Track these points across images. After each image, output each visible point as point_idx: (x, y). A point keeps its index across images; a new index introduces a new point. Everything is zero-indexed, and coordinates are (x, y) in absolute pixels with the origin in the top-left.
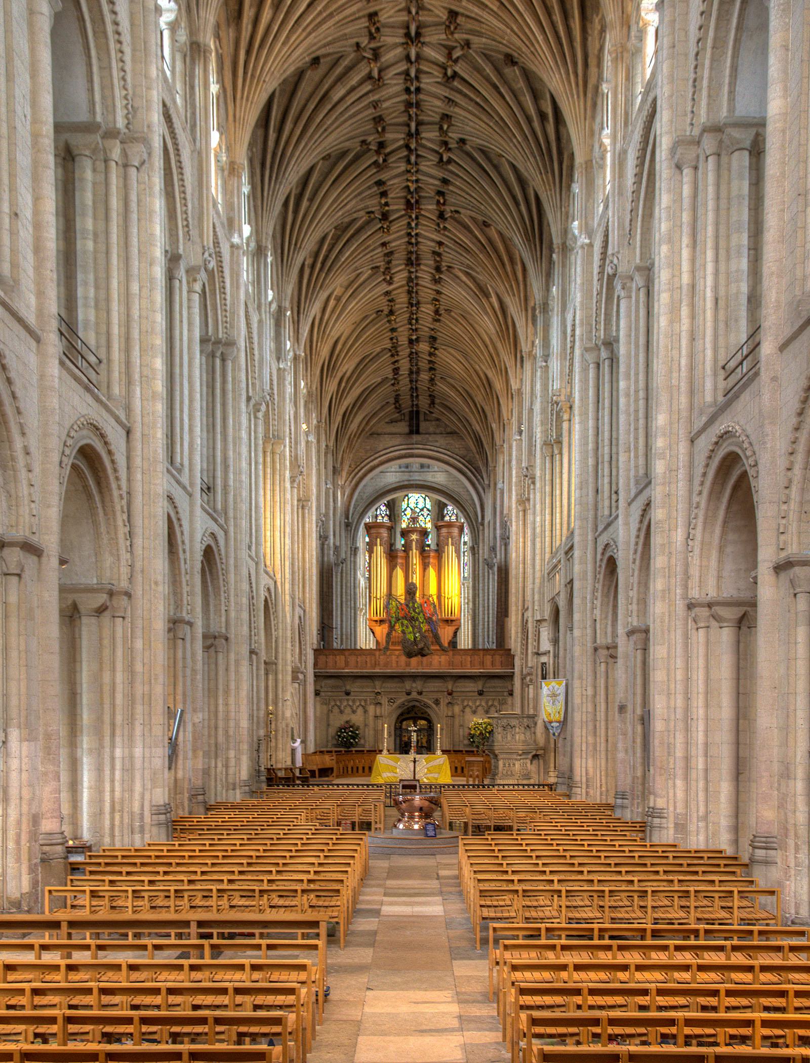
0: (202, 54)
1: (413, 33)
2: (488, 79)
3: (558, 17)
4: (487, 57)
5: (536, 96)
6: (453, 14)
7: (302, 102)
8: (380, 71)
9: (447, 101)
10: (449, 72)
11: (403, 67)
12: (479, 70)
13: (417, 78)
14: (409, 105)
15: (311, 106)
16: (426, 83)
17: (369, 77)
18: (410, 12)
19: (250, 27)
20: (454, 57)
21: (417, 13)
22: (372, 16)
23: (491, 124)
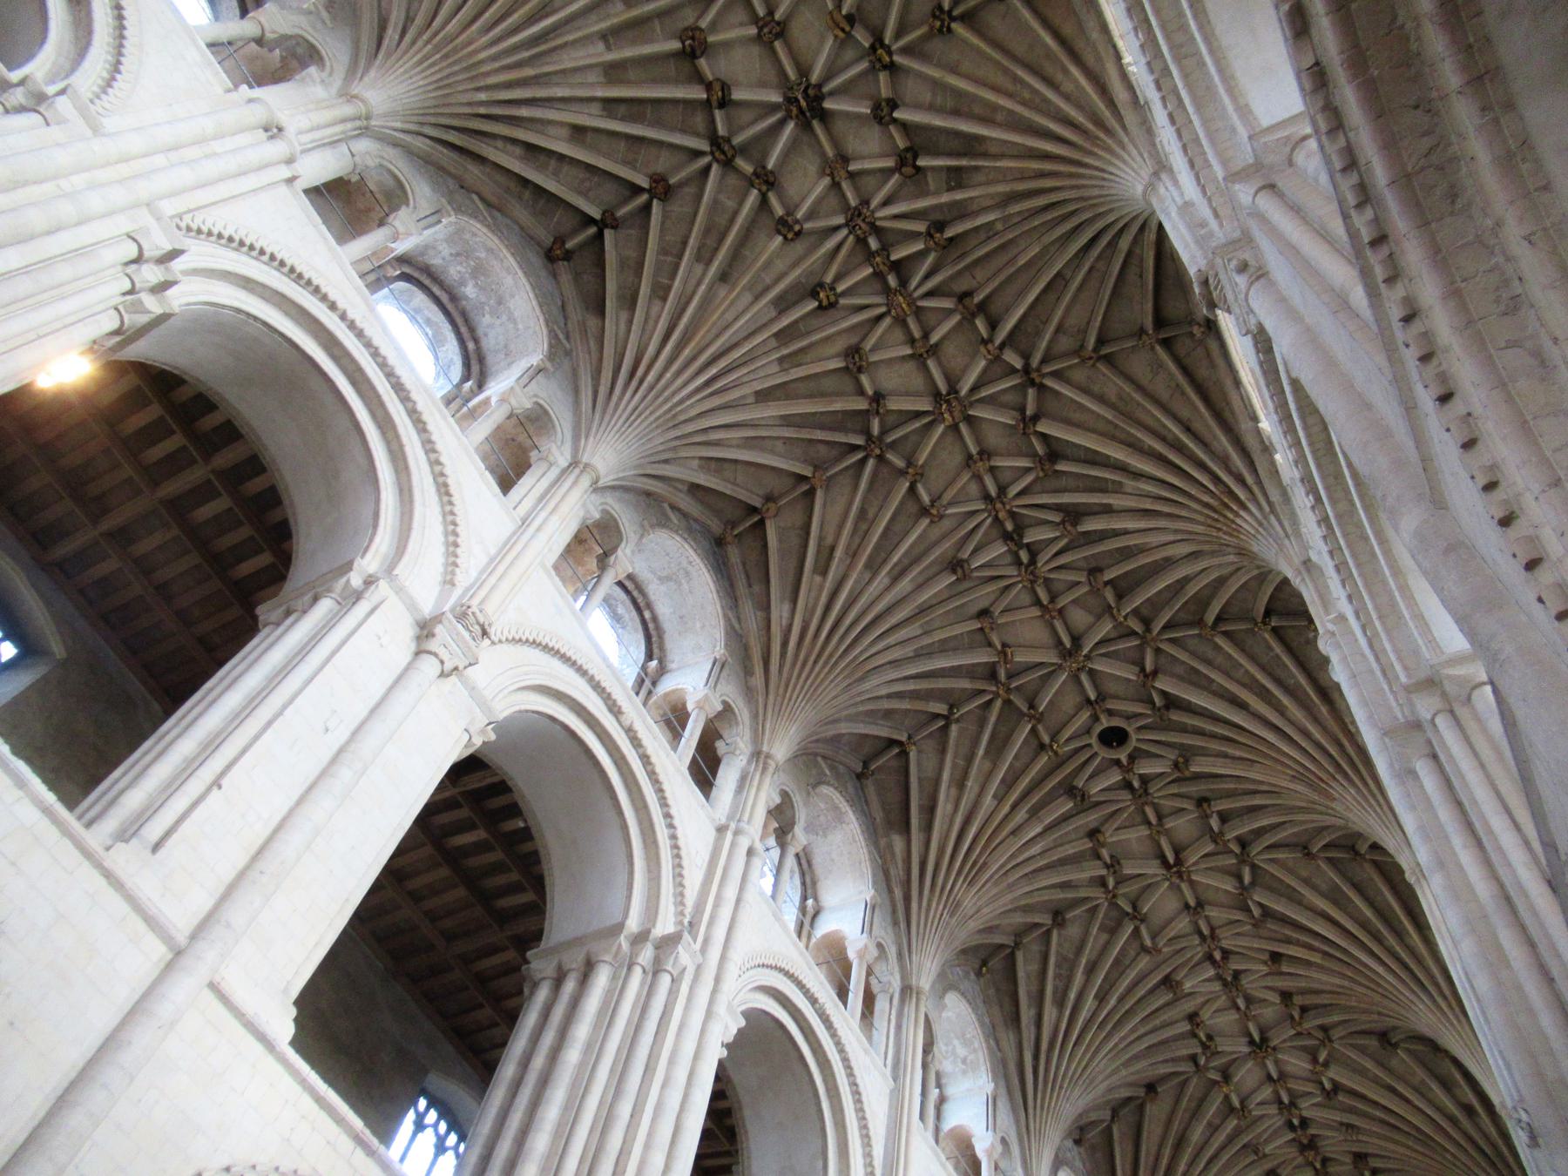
0: (914, 995)
1: (1257, 1038)
2: (1376, 1081)
3: (1391, 940)
4: (1362, 1050)
5: (1447, 1085)
6: (1286, 996)
7: (1154, 1150)
8: (1242, 1102)
9: (1344, 1129)
10: (1328, 1086)
11: (1266, 1092)
12: (1362, 1072)
13: (1293, 1104)
14: (1303, 1148)
15: (1167, 1152)
16: (1307, 1108)
17: (1229, 1110)
18: (1238, 1009)
19: (1033, 1029)
20: (1321, 1060)
21: (1247, 1007)
22: (1192, 1017)
23: (1410, 1143)
